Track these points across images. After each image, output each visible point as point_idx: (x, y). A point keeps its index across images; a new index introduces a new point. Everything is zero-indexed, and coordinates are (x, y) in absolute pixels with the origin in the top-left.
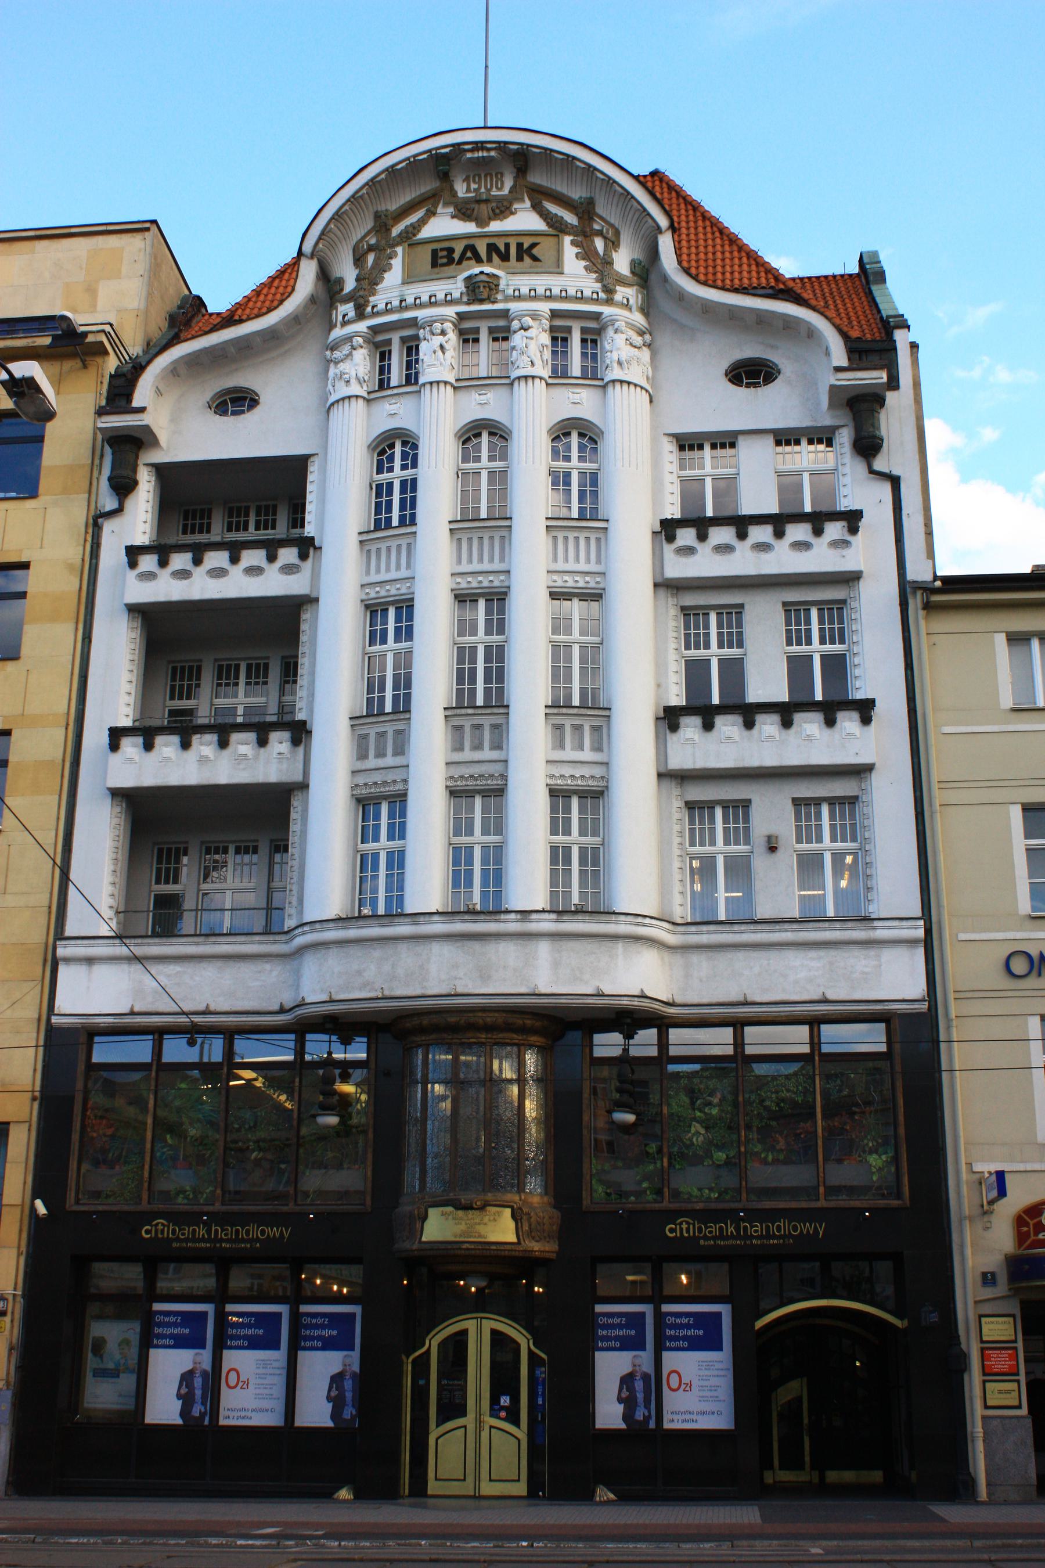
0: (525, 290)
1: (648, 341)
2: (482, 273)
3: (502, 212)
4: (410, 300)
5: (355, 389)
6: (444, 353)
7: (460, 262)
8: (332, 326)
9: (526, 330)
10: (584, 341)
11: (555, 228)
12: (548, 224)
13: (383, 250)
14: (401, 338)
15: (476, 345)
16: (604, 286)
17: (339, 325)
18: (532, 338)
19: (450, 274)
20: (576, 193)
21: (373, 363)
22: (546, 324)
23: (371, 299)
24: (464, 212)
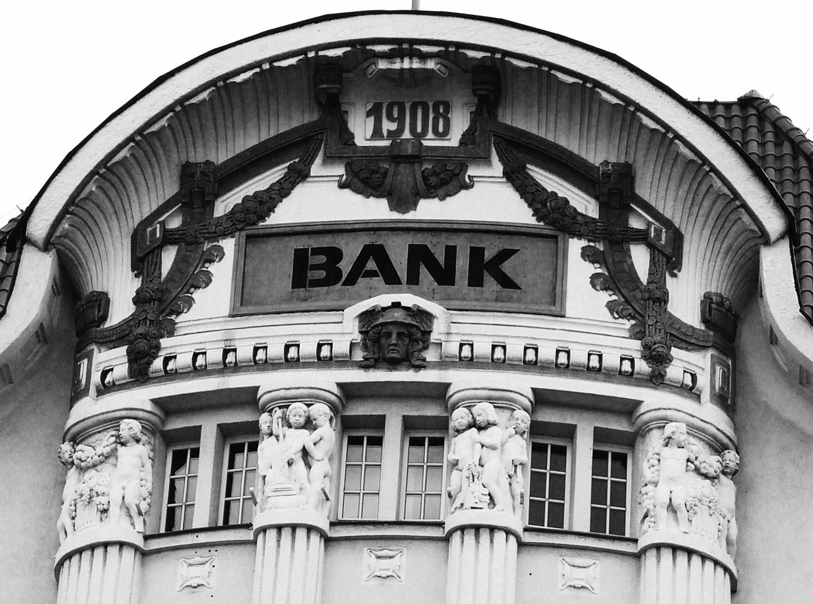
0: (482, 348)
1: (732, 465)
2: (396, 305)
3: (444, 183)
4: (244, 352)
5: (119, 528)
6: (309, 466)
7: (351, 280)
8: (77, 393)
9: (480, 428)
10: (599, 456)
11: (551, 223)
12: (536, 213)
13: (196, 246)
14: (220, 427)
15: (376, 449)
16: (646, 347)
17: (92, 391)
18: (493, 448)
19: (334, 304)
20: (597, 153)
21: (159, 475)
22: (523, 418)
23: (164, 342)
24: (364, 177)
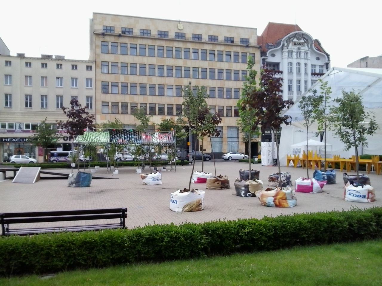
13: (289, 42)
24: (297, 39)
